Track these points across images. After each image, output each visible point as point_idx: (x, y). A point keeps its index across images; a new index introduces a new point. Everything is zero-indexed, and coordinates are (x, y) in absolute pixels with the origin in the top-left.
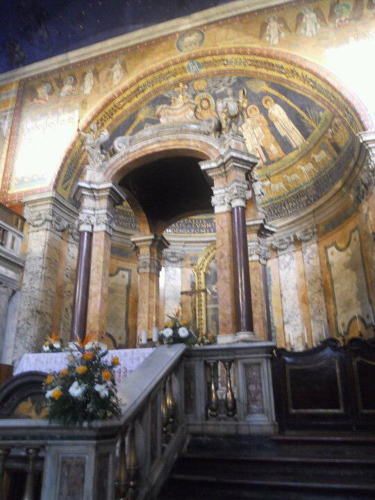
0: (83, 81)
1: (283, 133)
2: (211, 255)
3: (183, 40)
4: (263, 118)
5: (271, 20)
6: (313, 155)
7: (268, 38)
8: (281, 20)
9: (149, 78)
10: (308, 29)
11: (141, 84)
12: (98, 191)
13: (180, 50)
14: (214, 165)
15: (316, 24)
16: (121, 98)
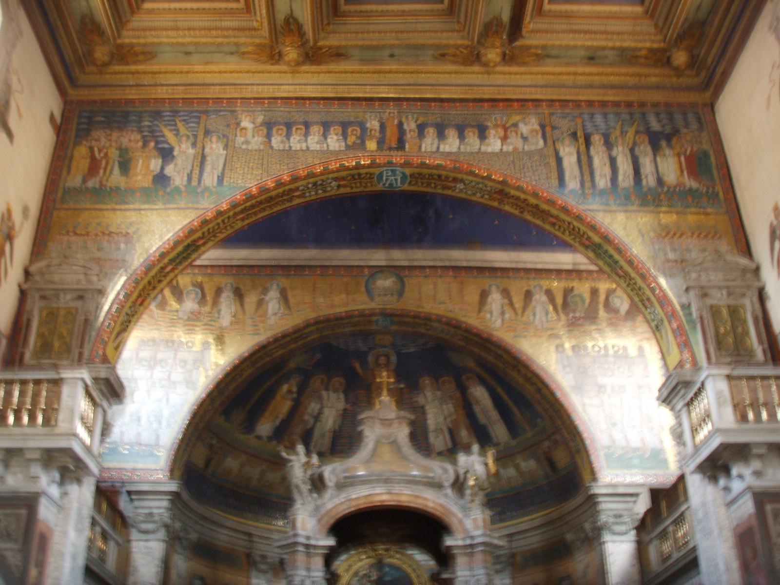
0: (216, 302)
1: (482, 420)
2: (355, 568)
3: (374, 283)
4: (458, 395)
5: (494, 289)
6: (517, 461)
7: (488, 316)
8: (506, 293)
9: (321, 326)
10: (538, 317)
11: (307, 331)
12: (315, 547)
13: (372, 298)
14: (460, 543)
15: (547, 314)
16: (277, 344)
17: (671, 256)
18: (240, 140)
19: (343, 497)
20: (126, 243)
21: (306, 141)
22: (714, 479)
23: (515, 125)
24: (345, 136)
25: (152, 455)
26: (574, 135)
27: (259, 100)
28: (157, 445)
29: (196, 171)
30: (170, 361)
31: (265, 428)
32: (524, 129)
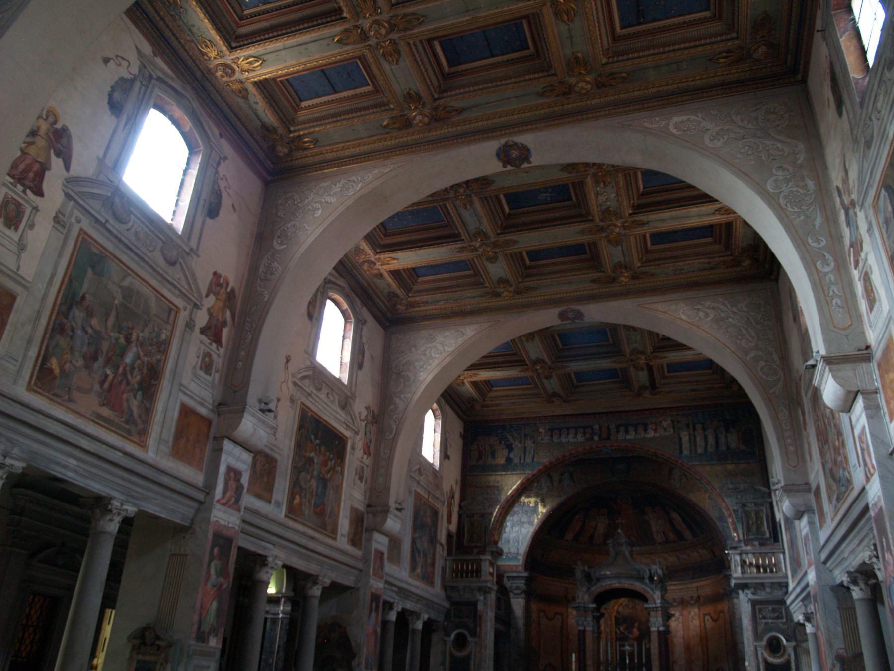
14: (651, 606)
17: (731, 486)
18: (540, 438)
19: (599, 584)
20: (498, 490)
21: (567, 437)
22: (743, 591)
23: (661, 422)
24: (584, 434)
25: (516, 558)
26: (688, 426)
27: (546, 417)
28: (518, 554)
29: (523, 456)
30: (521, 512)
31: (569, 536)
32: (664, 424)
